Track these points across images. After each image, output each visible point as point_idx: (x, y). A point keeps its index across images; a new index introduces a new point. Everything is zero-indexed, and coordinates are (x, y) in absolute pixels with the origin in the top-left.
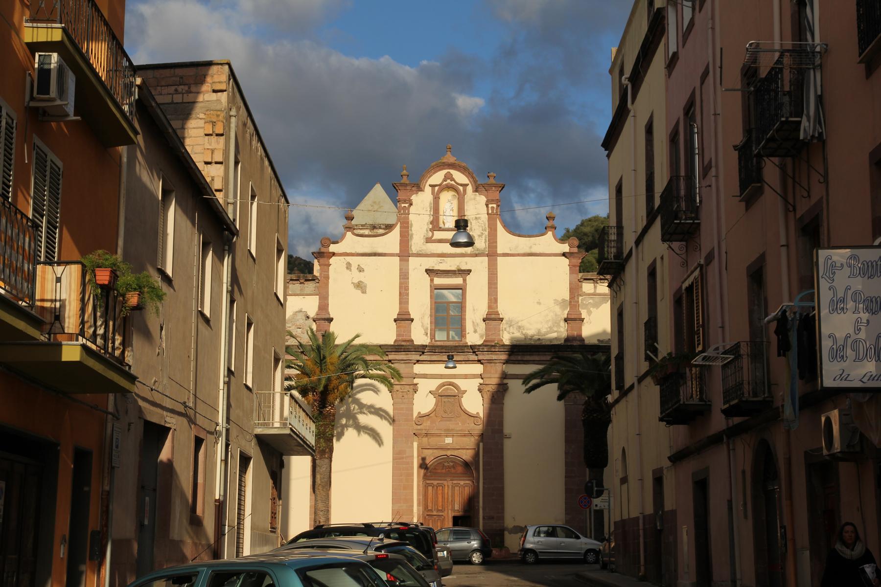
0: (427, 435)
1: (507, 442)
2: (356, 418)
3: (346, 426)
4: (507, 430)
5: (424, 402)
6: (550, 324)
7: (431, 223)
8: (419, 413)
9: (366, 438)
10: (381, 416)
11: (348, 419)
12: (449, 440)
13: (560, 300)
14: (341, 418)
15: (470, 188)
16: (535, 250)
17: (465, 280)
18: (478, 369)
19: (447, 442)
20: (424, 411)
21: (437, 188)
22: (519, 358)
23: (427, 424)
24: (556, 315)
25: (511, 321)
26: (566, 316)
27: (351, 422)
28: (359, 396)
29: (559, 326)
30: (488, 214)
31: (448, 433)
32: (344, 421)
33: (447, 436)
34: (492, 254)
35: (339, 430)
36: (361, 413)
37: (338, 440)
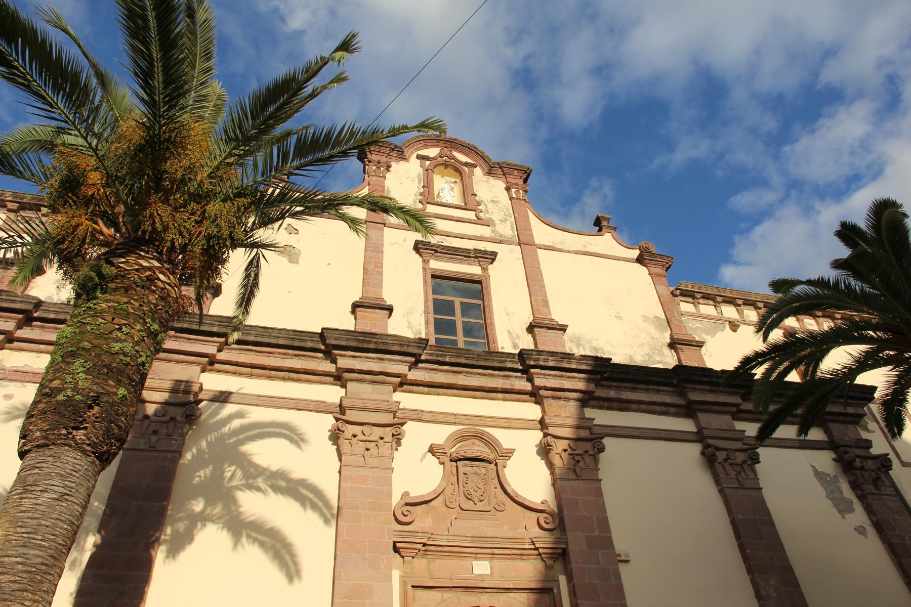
0: (427, 548)
1: (622, 567)
2: (235, 501)
3: (203, 518)
4: (620, 545)
5: (415, 470)
6: (646, 350)
7: (421, 194)
8: (406, 494)
9: (253, 555)
10: (303, 501)
11: (210, 502)
12: (481, 568)
13: (651, 317)
14: (195, 497)
15: (478, 171)
16: (590, 249)
17: (485, 270)
18: (532, 411)
19: (476, 571)
20: (419, 491)
21: (428, 163)
22: (612, 394)
23: (423, 521)
24: (652, 338)
25: (579, 338)
26: (669, 341)
27: (218, 509)
28: (250, 448)
29: (661, 354)
30: (510, 199)
31: (483, 548)
32: (198, 506)
33: (476, 556)
34: (524, 242)
35: (181, 527)
36: (250, 487)
37: (173, 552)
